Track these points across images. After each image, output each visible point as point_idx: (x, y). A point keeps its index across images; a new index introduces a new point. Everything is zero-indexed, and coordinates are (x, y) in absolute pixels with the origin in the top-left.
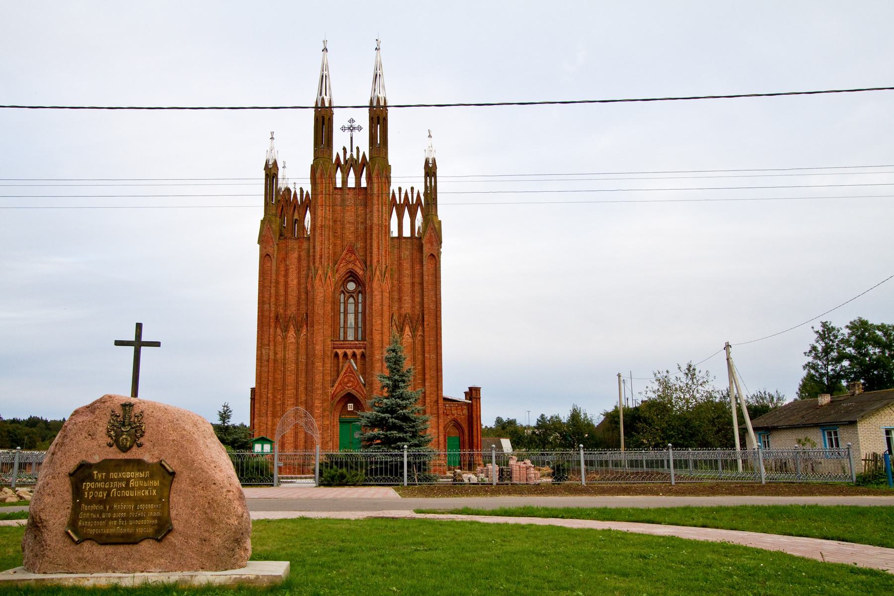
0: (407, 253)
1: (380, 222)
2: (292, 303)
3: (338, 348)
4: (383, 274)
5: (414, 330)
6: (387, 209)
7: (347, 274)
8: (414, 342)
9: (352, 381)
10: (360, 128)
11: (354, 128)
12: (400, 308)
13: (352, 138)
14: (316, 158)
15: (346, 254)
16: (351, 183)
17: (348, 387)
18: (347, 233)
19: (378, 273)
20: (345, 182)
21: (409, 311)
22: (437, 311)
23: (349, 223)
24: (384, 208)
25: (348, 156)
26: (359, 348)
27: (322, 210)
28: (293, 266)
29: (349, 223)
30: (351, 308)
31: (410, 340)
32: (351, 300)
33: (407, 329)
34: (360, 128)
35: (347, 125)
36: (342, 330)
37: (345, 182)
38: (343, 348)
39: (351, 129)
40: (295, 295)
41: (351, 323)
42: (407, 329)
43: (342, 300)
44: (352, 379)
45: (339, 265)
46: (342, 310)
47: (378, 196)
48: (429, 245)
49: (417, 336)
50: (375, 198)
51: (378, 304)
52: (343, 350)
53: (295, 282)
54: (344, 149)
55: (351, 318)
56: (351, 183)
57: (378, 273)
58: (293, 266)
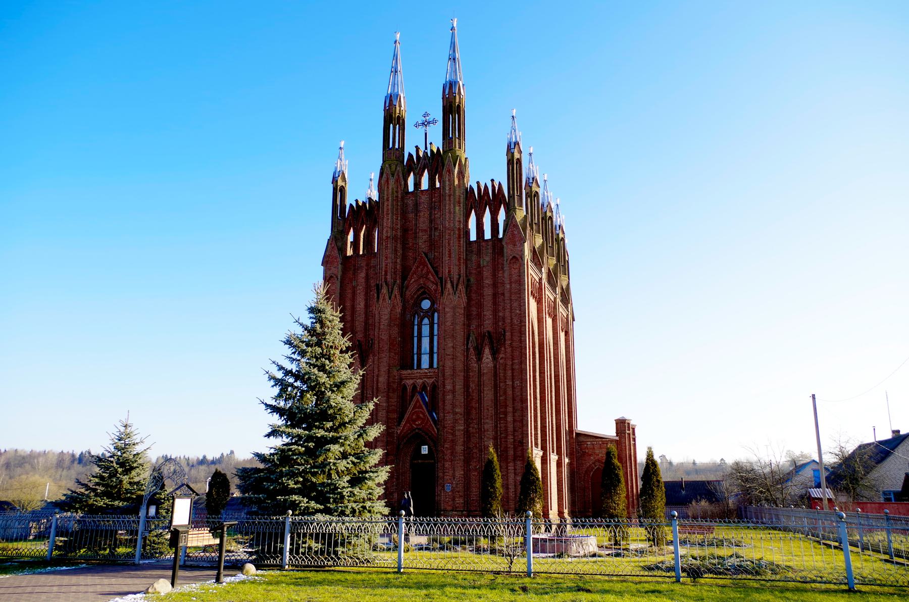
0: (487, 259)
1: (452, 225)
2: (359, 329)
3: (406, 379)
4: (455, 286)
5: (495, 353)
6: (462, 209)
7: (418, 290)
8: (495, 367)
9: (422, 418)
10: (434, 122)
11: (429, 123)
12: (480, 325)
13: (426, 134)
14: (384, 161)
15: (418, 267)
16: (425, 185)
17: (416, 425)
18: (421, 242)
19: (449, 285)
20: (417, 184)
21: (490, 329)
22: (521, 326)
23: (423, 231)
24: (457, 208)
25: (421, 154)
26: (430, 378)
27: (388, 219)
28: (361, 288)
29: (423, 231)
30: (426, 330)
31: (491, 365)
32: (426, 321)
33: (487, 351)
34: (434, 122)
35: (421, 119)
36: (415, 357)
37: (417, 184)
38: (412, 379)
39: (425, 124)
40: (361, 320)
41: (426, 348)
42: (487, 351)
43: (416, 323)
44: (421, 415)
45: (410, 281)
46: (416, 334)
47: (450, 196)
48: (511, 246)
49: (498, 358)
50: (447, 198)
51: (448, 324)
52: (411, 381)
53: (362, 305)
54: (417, 148)
55: (426, 342)
56: (425, 185)
57: (449, 285)
58: (361, 288)
